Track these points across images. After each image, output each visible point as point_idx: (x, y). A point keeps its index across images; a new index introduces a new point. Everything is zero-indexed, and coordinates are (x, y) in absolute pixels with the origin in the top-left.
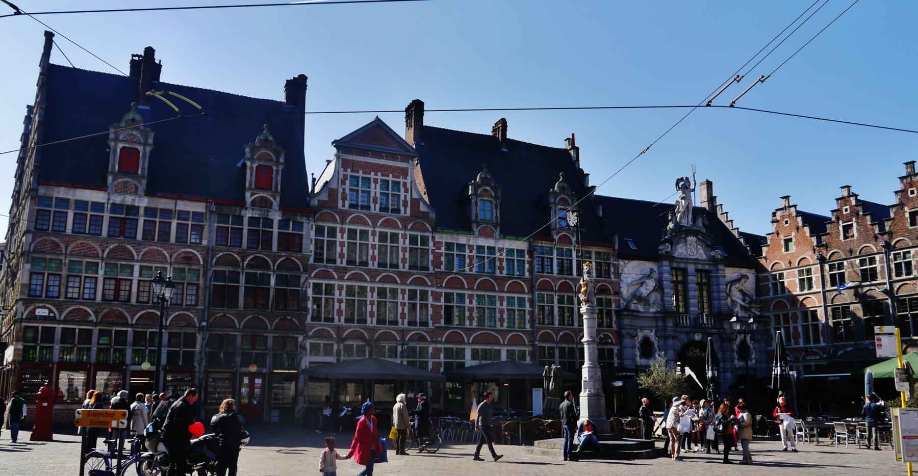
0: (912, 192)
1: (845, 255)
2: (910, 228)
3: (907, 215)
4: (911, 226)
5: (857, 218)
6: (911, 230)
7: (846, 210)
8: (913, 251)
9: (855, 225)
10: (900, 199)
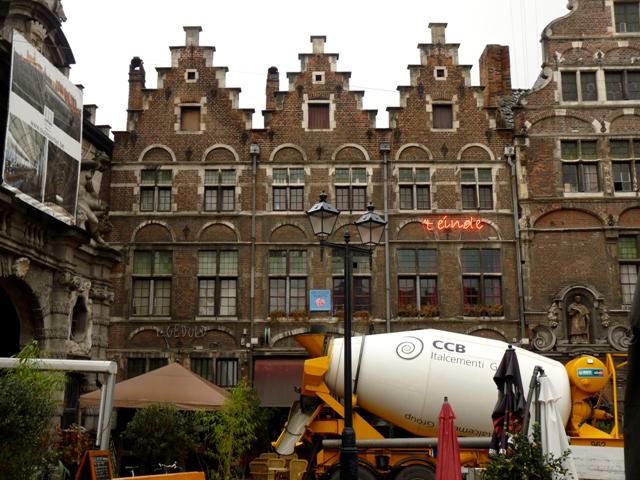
0: (440, 74)
1: (308, 155)
2: (433, 130)
3: (429, 108)
4: (434, 127)
5: (338, 96)
6: (433, 134)
7: (319, 78)
8: (433, 169)
9: (333, 107)
10: (419, 79)
